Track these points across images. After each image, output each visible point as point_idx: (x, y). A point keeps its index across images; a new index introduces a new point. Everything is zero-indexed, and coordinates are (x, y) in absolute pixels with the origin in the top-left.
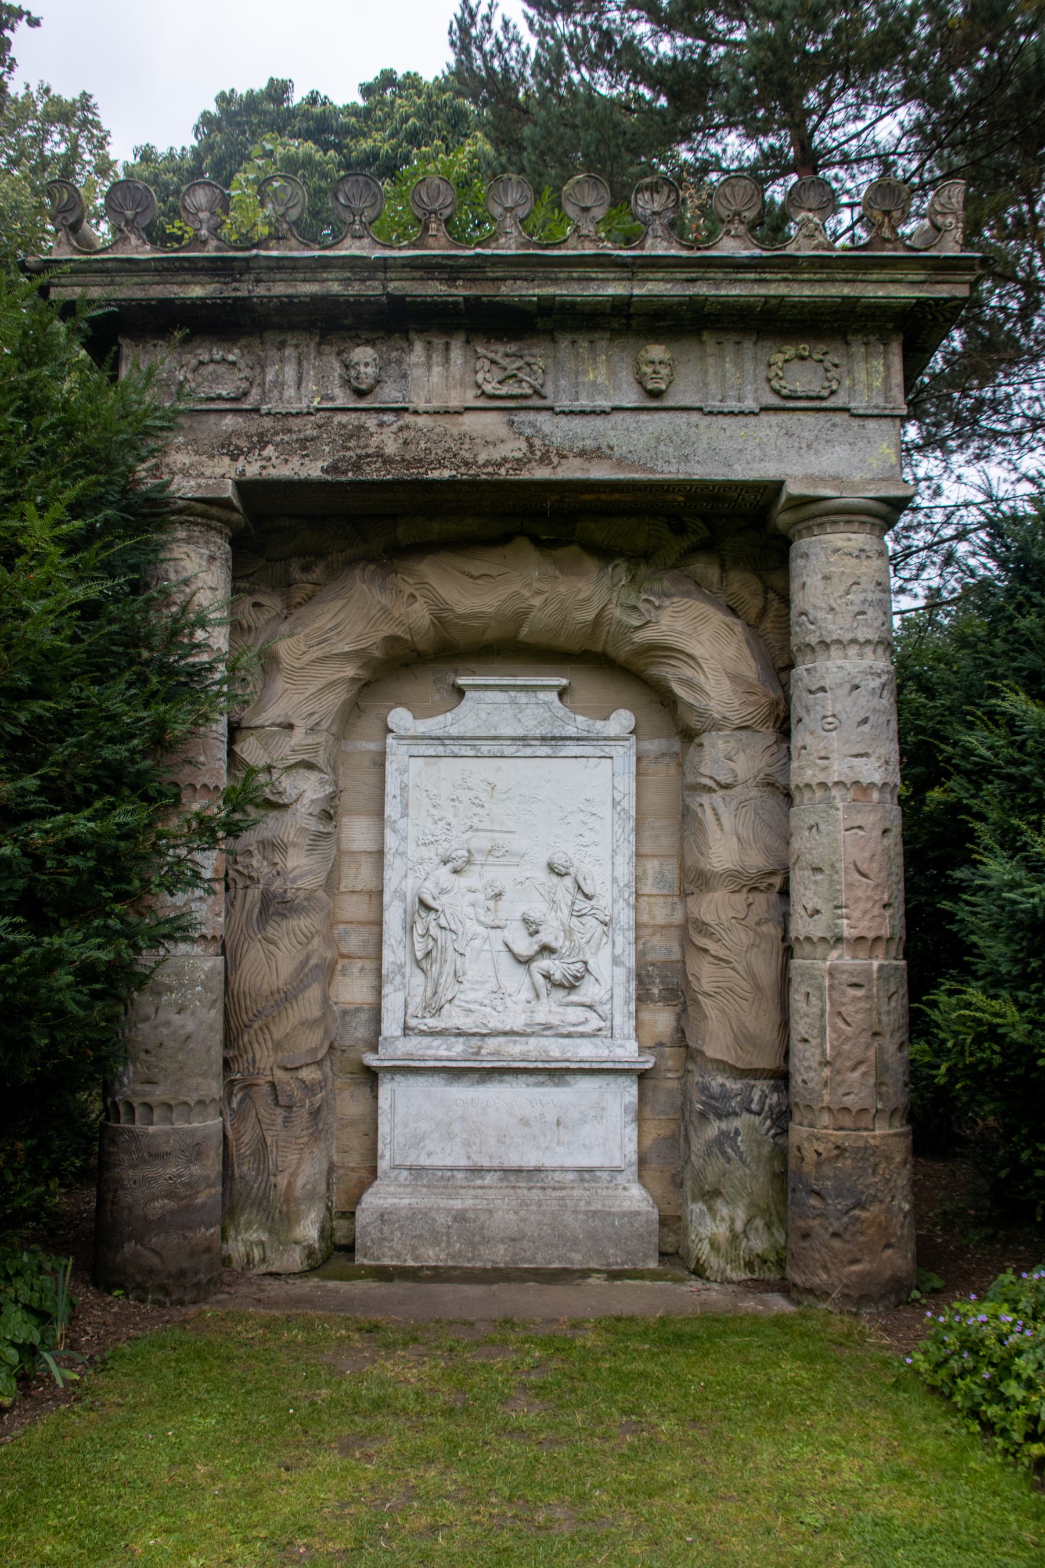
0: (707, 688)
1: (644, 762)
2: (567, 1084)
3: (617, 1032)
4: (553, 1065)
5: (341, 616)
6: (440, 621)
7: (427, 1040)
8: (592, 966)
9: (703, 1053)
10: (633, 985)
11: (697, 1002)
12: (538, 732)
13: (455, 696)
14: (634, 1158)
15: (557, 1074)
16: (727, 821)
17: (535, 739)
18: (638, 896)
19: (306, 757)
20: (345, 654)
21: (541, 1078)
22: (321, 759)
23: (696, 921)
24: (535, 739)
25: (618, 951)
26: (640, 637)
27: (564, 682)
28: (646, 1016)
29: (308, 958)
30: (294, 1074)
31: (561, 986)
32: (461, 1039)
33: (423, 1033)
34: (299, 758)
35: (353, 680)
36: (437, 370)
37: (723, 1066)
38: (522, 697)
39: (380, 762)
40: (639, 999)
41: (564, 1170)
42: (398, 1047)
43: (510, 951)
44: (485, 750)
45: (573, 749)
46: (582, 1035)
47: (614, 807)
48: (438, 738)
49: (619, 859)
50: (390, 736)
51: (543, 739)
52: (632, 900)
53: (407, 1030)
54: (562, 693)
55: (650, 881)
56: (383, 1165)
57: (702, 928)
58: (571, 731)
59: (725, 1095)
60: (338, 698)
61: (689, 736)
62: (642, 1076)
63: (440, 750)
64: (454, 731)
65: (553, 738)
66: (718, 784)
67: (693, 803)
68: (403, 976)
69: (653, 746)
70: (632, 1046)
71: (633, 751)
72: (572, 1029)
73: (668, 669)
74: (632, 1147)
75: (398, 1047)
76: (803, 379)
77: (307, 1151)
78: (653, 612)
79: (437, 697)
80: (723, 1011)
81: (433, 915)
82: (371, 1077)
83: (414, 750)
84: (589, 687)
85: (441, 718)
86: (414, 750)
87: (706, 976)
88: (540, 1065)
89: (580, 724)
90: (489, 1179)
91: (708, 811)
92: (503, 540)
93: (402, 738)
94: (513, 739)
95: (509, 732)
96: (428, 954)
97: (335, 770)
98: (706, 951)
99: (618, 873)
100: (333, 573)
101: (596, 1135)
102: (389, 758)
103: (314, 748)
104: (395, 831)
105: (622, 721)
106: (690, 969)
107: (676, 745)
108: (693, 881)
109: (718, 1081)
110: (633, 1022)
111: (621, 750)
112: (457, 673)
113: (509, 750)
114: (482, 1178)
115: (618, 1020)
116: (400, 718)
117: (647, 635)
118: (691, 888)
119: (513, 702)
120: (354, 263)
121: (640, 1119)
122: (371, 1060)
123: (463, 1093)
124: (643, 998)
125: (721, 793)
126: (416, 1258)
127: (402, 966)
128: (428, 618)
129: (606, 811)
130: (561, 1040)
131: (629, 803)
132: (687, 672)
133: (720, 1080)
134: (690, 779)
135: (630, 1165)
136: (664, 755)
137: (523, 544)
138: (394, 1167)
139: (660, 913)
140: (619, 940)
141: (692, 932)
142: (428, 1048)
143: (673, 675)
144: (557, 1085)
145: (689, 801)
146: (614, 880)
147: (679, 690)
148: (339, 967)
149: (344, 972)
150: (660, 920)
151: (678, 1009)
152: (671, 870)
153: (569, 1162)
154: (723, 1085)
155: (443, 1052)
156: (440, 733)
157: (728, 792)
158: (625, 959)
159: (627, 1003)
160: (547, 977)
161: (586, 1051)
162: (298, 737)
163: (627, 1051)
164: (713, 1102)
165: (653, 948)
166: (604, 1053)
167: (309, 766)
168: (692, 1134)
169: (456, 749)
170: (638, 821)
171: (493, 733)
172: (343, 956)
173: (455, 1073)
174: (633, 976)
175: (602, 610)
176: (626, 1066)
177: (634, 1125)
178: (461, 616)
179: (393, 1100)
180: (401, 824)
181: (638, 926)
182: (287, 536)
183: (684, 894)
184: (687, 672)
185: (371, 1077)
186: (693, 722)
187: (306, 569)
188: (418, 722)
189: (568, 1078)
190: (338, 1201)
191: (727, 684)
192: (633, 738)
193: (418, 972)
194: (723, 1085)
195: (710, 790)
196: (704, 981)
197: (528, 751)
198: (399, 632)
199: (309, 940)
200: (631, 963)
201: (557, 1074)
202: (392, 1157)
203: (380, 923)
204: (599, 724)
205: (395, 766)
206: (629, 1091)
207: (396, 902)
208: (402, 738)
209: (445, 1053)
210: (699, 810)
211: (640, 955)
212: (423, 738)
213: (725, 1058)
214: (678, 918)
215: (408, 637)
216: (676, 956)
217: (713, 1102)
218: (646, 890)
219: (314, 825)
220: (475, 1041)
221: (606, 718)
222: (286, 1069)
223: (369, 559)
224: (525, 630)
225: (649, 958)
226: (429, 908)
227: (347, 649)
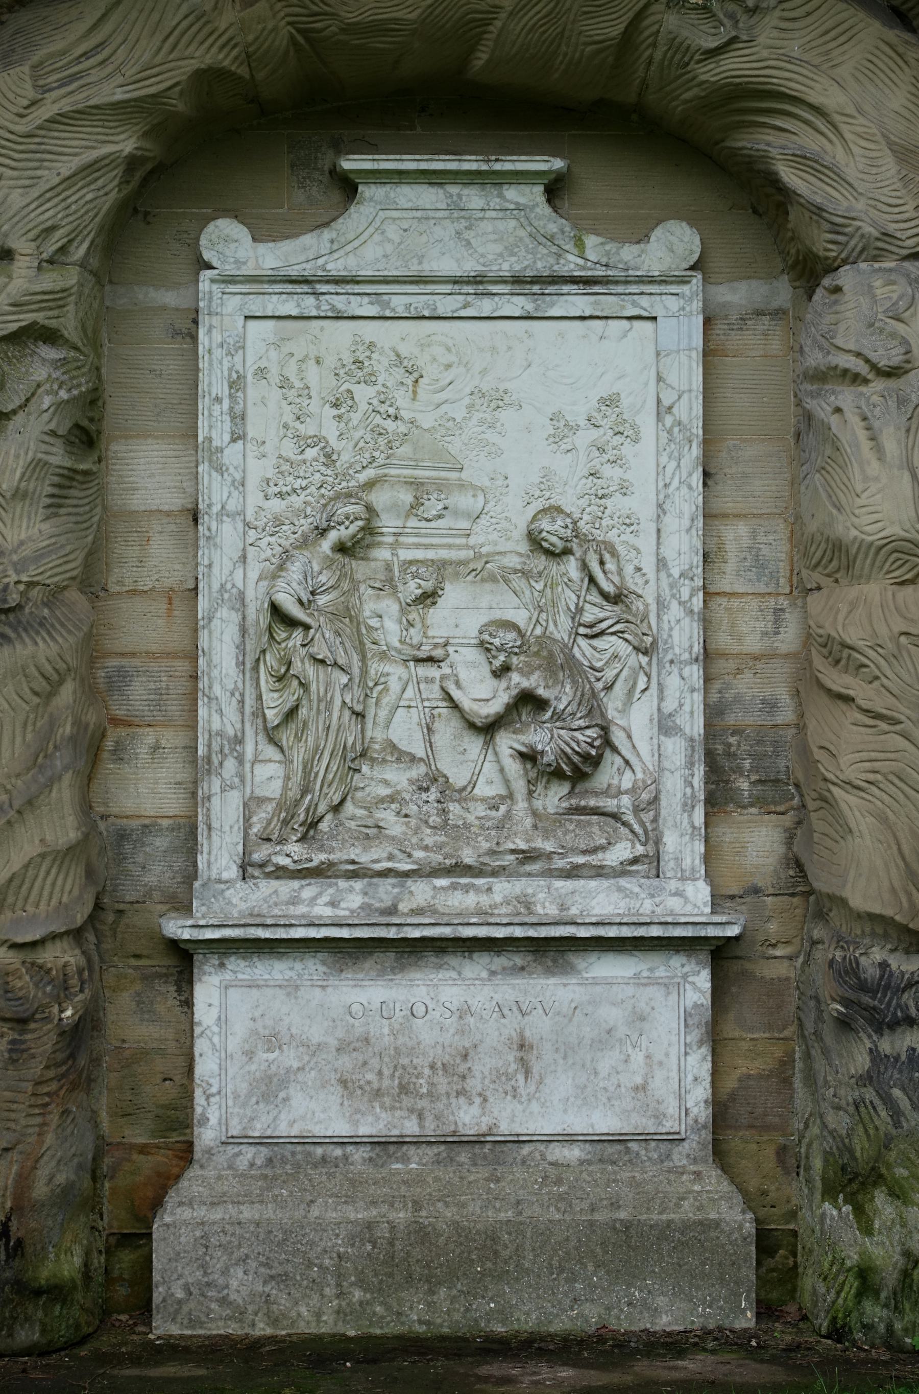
0: (851, 173)
1: (720, 328)
2: (568, 969)
3: (668, 866)
4: (543, 932)
5: (107, 28)
6: (309, 41)
7: (286, 887)
8: (618, 737)
9: (843, 902)
10: (700, 771)
11: (826, 801)
12: (506, 268)
13: (336, 196)
14: (701, 1112)
15: (551, 950)
16: (891, 444)
17: (502, 281)
18: (708, 595)
19: (39, 317)
20: (117, 107)
21: (518, 960)
22: (69, 325)
23: (827, 643)
24: (502, 281)
25: (669, 705)
26: (711, 73)
27: (558, 164)
28: (726, 833)
29: (53, 724)
30: (30, 956)
31: (557, 774)
32: (358, 885)
33: (281, 873)
34: (27, 318)
35: (132, 163)
37: (883, 927)
38: (473, 197)
39: (187, 329)
40: (711, 802)
41: (569, 1139)
42: (229, 899)
43: (454, 705)
44: (399, 304)
45: (578, 302)
46: (599, 872)
47: (659, 417)
48: (305, 281)
49: (671, 523)
50: (209, 273)
51: (517, 280)
52: (698, 602)
54: (555, 189)
55: (730, 567)
56: (206, 1136)
57: (839, 652)
58: (571, 264)
59: (887, 984)
60: (104, 194)
61: (811, 273)
62: (721, 954)
63: (309, 305)
64: (336, 267)
65: (536, 280)
66: (874, 367)
67: (821, 409)
68: (240, 760)
69: (737, 295)
70: (700, 893)
71: (697, 305)
72: (581, 860)
73: (771, 137)
74: (699, 1096)
75: (229, 899)
77: (55, 1111)
78: (743, 18)
79: (300, 196)
80: (883, 820)
81: (298, 636)
82: (183, 959)
83: (256, 306)
85: (308, 239)
86: (256, 306)
87: (848, 748)
88: (518, 932)
90: (415, 1162)
91: (854, 420)
93: (231, 280)
94: (456, 281)
95: (446, 266)
96: (291, 713)
97: (95, 344)
98: (848, 699)
99: (668, 552)
102: (205, 321)
103: (56, 299)
104: (220, 469)
105: (673, 243)
106: (816, 735)
107: (783, 292)
108: (824, 560)
109: (875, 956)
110: (700, 848)
111: (673, 304)
112: (340, 148)
113: (446, 305)
114: (406, 1160)
115: (671, 841)
117: (732, 67)
118: (817, 577)
119: (456, 208)
121: (716, 1040)
122: (177, 928)
124: (718, 798)
125: (879, 385)
126: (274, 1322)
127: (239, 740)
128: (286, 31)
130: (559, 884)
131: (690, 410)
132: (809, 141)
133: (878, 954)
134: (815, 359)
135: (697, 1127)
136: (759, 313)
138: (229, 1141)
139: (748, 630)
140: (673, 682)
141: (818, 662)
142: (294, 901)
143: (778, 146)
144: (549, 972)
145: (811, 404)
146: (661, 563)
147: (789, 176)
148: (109, 744)
149: (119, 753)
150: (753, 643)
151: (788, 820)
152: (776, 546)
153: (578, 1124)
154: (884, 965)
155: (323, 911)
156: (308, 270)
157: (892, 383)
158: (682, 720)
159: (688, 807)
160: (529, 757)
163: (687, 901)
164: (866, 999)
165: (738, 699)
166: (647, 907)
167: (50, 336)
168: (820, 1064)
169: (340, 302)
170: (709, 441)
171: (414, 269)
172: (116, 722)
173: (346, 952)
174: (699, 755)
175: (640, 16)
176: (688, 932)
177: (705, 1050)
178: (349, 29)
179: (224, 1007)
180: (232, 454)
181: (708, 656)
183: (802, 591)
184: (809, 141)
185: (183, 959)
186: (821, 242)
188: (262, 248)
189: (573, 958)
190: (113, 1217)
191: (889, 167)
192: (697, 279)
193: (271, 752)
194: (884, 965)
195: (856, 379)
196: (844, 760)
197: (486, 306)
198: (226, 60)
199: (55, 686)
200: (696, 726)
202: (225, 1122)
203: (192, 654)
204: (628, 253)
205: (217, 337)
206: (699, 982)
207: (224, 612)
208: (231, 280)
209: (328, 912)
210: (834, 420)
211: (714, 713)
212: (273, 280)
213: (889, 912)
214: (789, 638)
215: (243, 71)
216: (786, 715)
217: (866, 999)
218: (724, 584)
219: (59, 457)
220: (386, 890)
221: (643, 238)
222: (15, 946)
224: (481, 58)
225: (731, 719)
226: (291, 623)
227: (119, 96)
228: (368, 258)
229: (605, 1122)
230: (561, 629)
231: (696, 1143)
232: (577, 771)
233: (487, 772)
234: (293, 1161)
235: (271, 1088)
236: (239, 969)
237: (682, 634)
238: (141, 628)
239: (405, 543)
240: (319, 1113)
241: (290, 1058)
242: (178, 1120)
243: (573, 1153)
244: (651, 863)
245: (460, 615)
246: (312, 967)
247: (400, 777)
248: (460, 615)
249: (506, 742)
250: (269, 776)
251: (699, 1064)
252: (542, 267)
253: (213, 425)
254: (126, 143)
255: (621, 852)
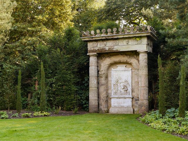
15: (125, 98)
35: (108, 67)
36: (111, 43)
38: (122, 67)
45: (126, 71)
53: (113, 95)
54: (126, 66)
58: (126, 70)
60: (107, 68)
76: (139, 41)
84: (128, 66)
89: (127, 69)
92: (119, 55)
100: (106, 58)
101: (128, 103)
112: (117, 65)
116: (112, 69)
120: (103, 37)
122: (110, 97)
123: (118, 100)
129: (129, 76)
137: (120, 55)
153: (126, 105)
161: (127, 96)
162: (103, 71)
182: (101, 55)
187: (104, 58)
200: (131, 89)
201: (125, 98)
204: (128, 69)
223: (108, 57)
228: (118, 70)
229: (127, 105)
230: (126, 85)
231: (131, 106)
232: (127, 91)
233: (123, 91)
234: (115, 107)
235: (114, 104)
236: (113, 99)
237: (131, 85)
238: (109, 85)
239: (120, 81)
240: (116, 105)
241: (115, 102)
242: (111, 105)
243: (126, 107)
244: (130, 94)
245: (122, 84)
246: (116, 99)
247: (119, 91)
248: (122, 84)
249: (123, 90)
250: (114, 91)
251: (131, 103)
252: (125, 70)
253: (112, 77)
254: (108, 66)
255: (128, 94)
